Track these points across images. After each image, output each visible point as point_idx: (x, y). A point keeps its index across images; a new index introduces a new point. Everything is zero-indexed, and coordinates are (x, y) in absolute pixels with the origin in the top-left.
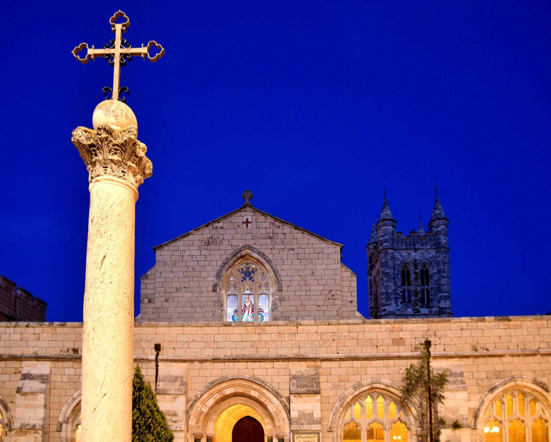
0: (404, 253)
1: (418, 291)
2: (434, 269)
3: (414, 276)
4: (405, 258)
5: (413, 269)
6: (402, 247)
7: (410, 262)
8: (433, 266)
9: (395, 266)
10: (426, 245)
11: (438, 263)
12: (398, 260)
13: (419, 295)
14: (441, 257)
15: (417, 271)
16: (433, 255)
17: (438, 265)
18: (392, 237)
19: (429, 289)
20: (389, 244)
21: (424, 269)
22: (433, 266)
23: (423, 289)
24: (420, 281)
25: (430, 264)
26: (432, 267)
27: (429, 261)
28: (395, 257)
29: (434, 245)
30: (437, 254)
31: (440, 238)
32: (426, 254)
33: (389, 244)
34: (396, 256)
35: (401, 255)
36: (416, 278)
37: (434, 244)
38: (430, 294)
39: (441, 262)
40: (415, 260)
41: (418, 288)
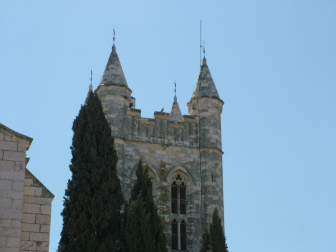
0: (144, 149)
1: (167, 223)
2: (196, 185)
3: (159, 193)
4: (143, 157)
5: (158, 179)
6: (140, 138)
7: (153, 167)
8: (193, 180)
9: (125, 170)
10: (182, 139)
11: (204, 174)
12: (131, 160)
13: (166, 231)
14: (207, 164)
15: (165, 184)
16: (194, 160)
17: (203, 178)
18: (122, 117)
19: (186, 221)
20: (117, 129)
21: (179, 182)
22: (193, 180)
23: (175, 220)
24: (169, 204)
25: (188, 174)
26: (191, 181)
27: (186, 169)
28: (126, 153)
29: (196, 140)
30: (202, 157)
31: (208, 131)
32: (182, 155)
33: (117, 129)
34: (128, 151)
35: (137, 151)
36: (164, 198)
37: (196, 139)
38: (187, 231)
39: (207, 174)
40: (163, 165)
41: (166, 216)
